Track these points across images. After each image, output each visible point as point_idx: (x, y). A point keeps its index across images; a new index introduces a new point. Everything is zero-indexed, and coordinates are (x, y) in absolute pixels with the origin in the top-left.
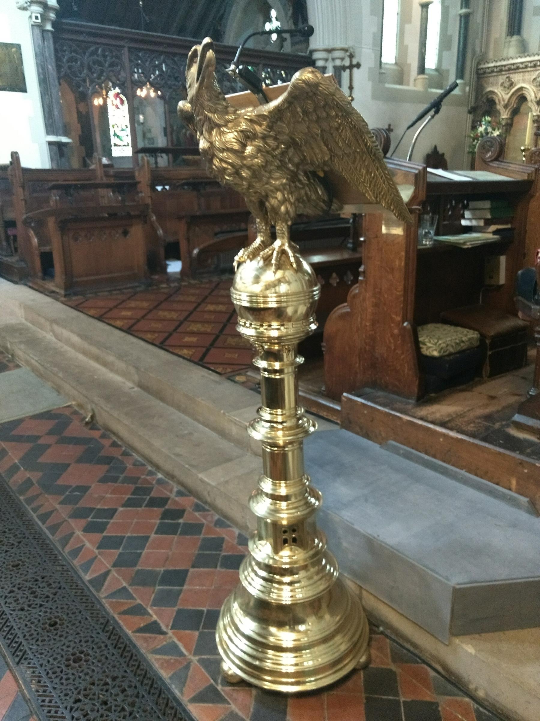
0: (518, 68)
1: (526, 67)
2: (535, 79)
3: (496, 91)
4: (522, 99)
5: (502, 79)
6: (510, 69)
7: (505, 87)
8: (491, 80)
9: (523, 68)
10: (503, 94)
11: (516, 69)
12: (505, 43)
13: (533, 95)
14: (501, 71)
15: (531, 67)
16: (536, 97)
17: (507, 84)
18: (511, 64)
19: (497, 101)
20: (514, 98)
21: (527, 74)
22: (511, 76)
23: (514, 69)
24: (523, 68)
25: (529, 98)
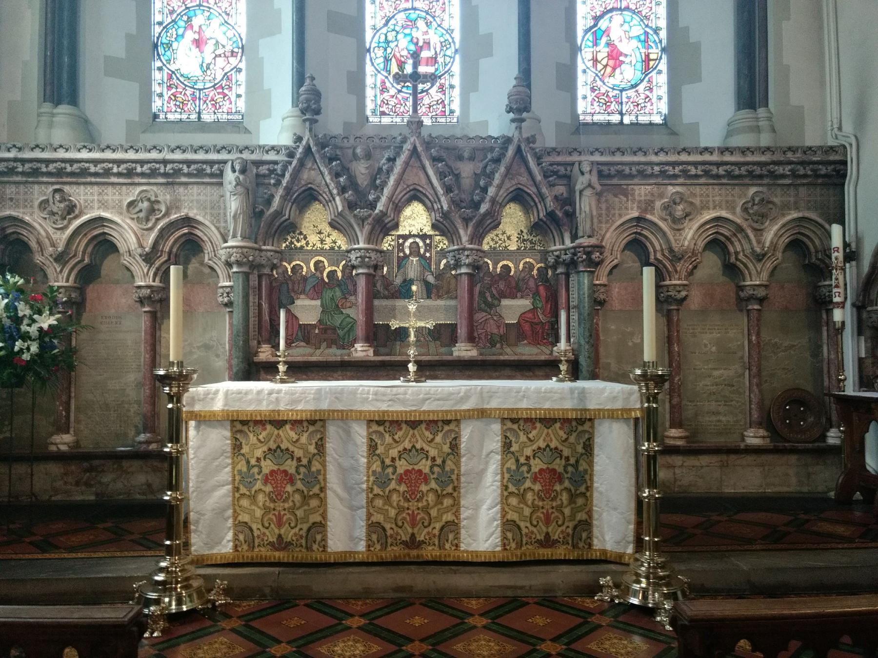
0: (84, 173)
1: (107, 173)
2: (131, 204)
3: (27, 218)
4: (105, 246)
5: (40, 192)
6: (60, 173)
7: (53, 214)
8: (10, 190)
9: (96, 174)
10: (51, 231)
11: (81, 174)
12: (39, 115)
13: (132, 240)
14: (36, 172)
15: (119, 175)
16: (141, 246)
17: (58, 207)
18: (64, 161)
19: (33, 244)
20: (81, 244)
21: (110, 189)
22: (67, 188)
23: (72, 174)
24: (96, 174)
25: (122, 247)
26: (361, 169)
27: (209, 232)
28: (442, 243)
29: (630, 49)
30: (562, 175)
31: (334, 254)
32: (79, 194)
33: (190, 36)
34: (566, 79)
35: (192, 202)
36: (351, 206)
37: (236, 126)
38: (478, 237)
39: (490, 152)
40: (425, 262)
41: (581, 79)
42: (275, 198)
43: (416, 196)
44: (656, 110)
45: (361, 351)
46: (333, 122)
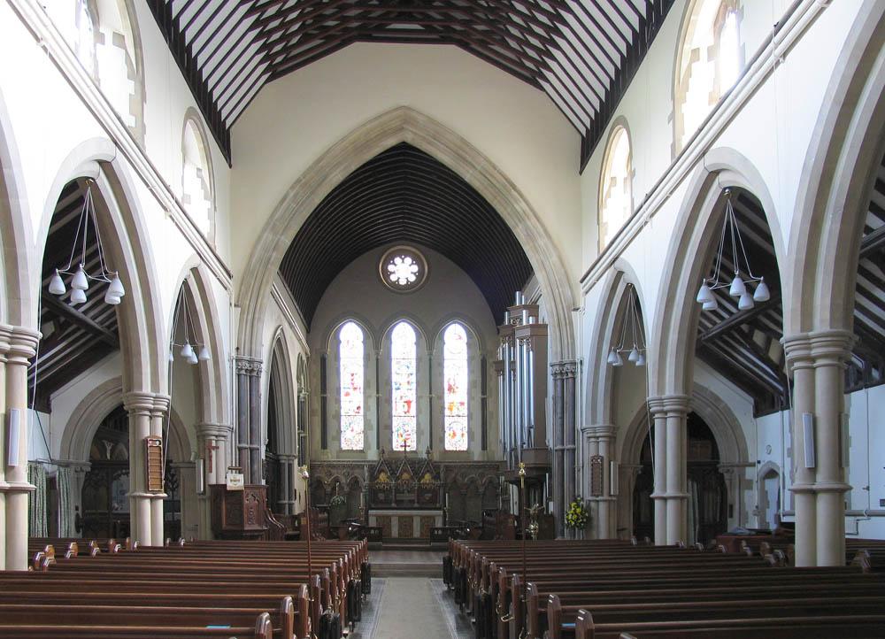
26: (394, 466)
27: (361, 479)
28: (411, 481)
29: (459, 433)
30: (439, 467)
31: (387, 484)
32: (333, 471)
33: (350, 429)
34: (442, 440)
35: (357, 473)
36: (391, 474)
37: (361, 451)
38: (419, 480)
39: (421, 461)
40: (408, 486)
41: (446, 440)
42: (374, 470)
43: (405, 471)
44: (464, 447)
45: (393, 505)
46: (386, 456)
